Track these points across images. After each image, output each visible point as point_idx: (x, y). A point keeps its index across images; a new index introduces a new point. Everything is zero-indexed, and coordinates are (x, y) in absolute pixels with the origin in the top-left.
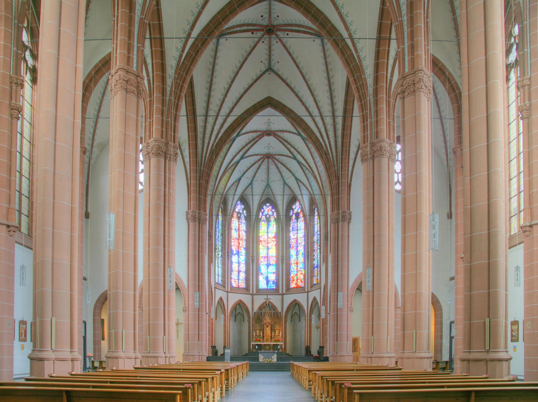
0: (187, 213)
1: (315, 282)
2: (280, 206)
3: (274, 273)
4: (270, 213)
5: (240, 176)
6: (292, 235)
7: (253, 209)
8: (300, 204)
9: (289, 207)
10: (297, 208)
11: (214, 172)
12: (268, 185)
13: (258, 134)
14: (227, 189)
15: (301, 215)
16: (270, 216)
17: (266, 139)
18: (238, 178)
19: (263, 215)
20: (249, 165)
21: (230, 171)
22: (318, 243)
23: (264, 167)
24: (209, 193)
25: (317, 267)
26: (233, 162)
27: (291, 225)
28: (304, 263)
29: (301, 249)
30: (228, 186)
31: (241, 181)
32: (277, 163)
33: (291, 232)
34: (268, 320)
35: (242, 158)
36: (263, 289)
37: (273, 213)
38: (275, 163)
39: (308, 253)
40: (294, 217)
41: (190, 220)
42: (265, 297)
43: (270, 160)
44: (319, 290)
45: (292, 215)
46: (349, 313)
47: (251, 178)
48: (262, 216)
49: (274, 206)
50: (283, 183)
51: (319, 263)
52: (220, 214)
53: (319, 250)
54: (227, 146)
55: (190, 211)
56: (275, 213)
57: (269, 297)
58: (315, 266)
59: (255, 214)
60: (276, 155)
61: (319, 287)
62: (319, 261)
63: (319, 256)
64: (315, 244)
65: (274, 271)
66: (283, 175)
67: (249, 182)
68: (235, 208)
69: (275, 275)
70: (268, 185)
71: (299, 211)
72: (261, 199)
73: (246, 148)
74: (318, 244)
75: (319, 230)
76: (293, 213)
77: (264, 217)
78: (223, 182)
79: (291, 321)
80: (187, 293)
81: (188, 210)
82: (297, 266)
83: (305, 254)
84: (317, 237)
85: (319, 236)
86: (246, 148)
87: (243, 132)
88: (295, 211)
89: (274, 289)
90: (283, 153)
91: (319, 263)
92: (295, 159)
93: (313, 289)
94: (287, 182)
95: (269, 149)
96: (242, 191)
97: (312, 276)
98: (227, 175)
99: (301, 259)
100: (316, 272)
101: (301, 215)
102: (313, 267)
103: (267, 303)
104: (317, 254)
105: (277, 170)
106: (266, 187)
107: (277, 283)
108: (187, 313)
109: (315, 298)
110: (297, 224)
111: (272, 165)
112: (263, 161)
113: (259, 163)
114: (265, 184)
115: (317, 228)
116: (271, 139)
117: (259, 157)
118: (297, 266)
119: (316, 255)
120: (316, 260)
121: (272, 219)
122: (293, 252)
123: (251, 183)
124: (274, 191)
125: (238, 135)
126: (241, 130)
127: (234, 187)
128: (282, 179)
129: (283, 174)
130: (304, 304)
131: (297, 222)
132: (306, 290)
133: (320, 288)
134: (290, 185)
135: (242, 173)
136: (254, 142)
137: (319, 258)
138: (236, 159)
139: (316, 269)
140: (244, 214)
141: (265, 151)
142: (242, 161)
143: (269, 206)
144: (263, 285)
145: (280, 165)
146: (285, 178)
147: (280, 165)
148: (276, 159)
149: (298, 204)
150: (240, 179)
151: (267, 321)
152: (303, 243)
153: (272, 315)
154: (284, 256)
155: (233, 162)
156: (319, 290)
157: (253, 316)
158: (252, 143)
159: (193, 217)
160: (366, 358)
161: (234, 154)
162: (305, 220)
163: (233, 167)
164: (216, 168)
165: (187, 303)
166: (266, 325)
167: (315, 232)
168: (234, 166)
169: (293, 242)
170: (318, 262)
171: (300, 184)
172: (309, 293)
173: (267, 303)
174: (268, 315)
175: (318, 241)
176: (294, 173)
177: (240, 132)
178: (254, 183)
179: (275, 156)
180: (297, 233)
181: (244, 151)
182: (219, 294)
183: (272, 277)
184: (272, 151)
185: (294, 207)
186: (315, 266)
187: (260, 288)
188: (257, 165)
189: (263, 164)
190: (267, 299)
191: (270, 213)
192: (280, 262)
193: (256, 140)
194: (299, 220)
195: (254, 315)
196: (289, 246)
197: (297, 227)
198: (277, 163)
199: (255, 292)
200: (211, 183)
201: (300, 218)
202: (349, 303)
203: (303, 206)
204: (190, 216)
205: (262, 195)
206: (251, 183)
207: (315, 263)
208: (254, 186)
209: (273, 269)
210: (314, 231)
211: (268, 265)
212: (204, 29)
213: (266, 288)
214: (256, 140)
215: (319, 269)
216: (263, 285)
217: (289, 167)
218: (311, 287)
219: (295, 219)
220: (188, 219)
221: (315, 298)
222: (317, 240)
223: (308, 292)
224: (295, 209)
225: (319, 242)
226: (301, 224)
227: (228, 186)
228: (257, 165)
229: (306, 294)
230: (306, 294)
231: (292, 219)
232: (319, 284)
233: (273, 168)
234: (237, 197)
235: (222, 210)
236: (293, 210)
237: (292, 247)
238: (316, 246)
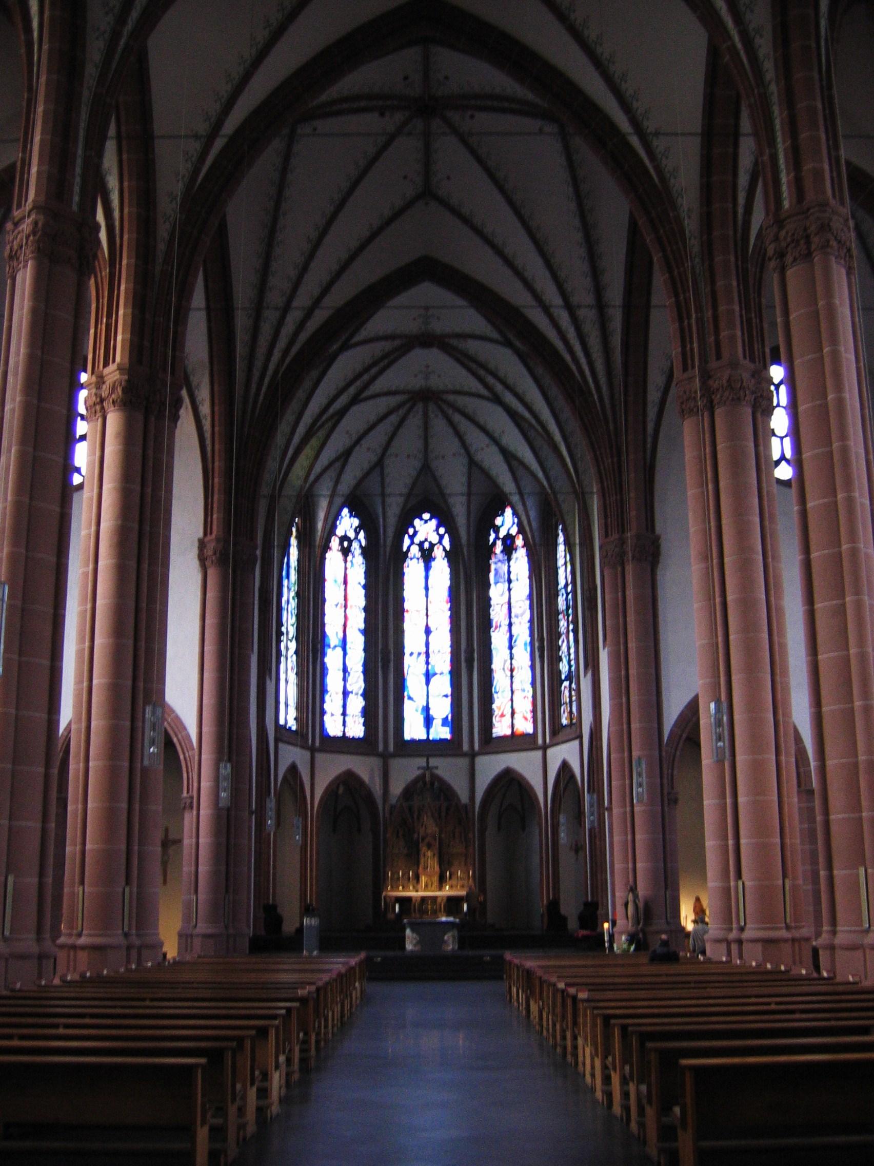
0: (202, 544)
1: (564, 721)
2: (461, 521)
3: (446, 696)
4: (434, 539)
5: (348, 443)
6: (497, 593)
7: (384, 527)
8: (515, 513)
9: (486, 523)
10: (507, 522)
11: (280, 439)
12: (426, 469)
13: (397, 342)
14: (312, 477)
15: (519, 542)
16: (432, 546)
17: (419, 357)
18: (341, 450)
19: (412, 543)
20: (373, 418)
21: (321, 434)
22: (568, 616)
23: (414, 422)
24: (265, 490)
25: (569, 677)
26: (331, 411)
27: (493, 567)
28: (533, 667)
29: (522, 631)
30: (318, 469)
31: (352, 459)
32: (450, 412)
33: (493, 586)
34: (429, 826)
35: (355, 400)
36: (413, 741)
37: (441, 537)
38: (443, 412)
39: (541, 640)
40: (499, 547)
41: (208, 563)
42: (422, 762)
43: (432, 407)
44: (577, 742)
45: (494, 543)
46: (666, 809)
47: (379, 451)
48: (409, 548)
49: (445, 519)
50: (465, 461)
51: (573, 669)
52: (293, 541)
53: (571, 635)
54: (314, 374)
55: (208, 538)
56: (446, 536)
57: (433, 762)
58: (563, 677)
59: (389, 541)
60: (447, 392)
61: (578, 733)
62: (573, 663)
63: (572, 650)
64: (561, 617)
65: (448, 691)
66: (468, 442)
67: (374, 458)
68: (334, 527)
69: (449, 700)
70: (426, 469)
71: (514, 531)
72: (406, 502)
73: (366, 377)
74: (570, 618)
75: (569, 581)
76: (497, 538)
77: (415, 550)
78: (303, 461)
79: (499, 829)
80: (196, 758)
81: (205, 534)
82: (512, 677)
83: (532, 643)
84: (567, 599)
85: (570, 596)
86: (366, 377)
87: (357, 338)
88: (503, 533)
89: (446, 740)
90: (466, 389)
91: (573, 669)
92: (497, 400)
93: (561, 737)
94: (478, 457)
95: (427, 378)
96: (353, 482)
97: (555, 703)
98: (314, 442)
99: (523, 657)
100: (567, 693)
101: (519, 542)
102: (555, 680)
103: (428, 779)
104: (566, 646)
105: (451, 431)
106: (421, 470)
107: (454, 722)
108: (195, 812)
109: (565, 766)
110: (509, 567)
111: (437, 416)
112: (411, 408)
113: (401, 412)
114: (417, 464)
115: (563, 576)
116: (434, 357)
117: (399, 399)
118: (512, 677)
119: (564, 648)
120: (565, 661)
121: (438, 553)
122: (498, 639)
123: (379, 464)
124: (444, 482)
125: (345, 347)
126: (352, 335)
127: (332, 473)
128: (462, 451)
129: (468, 439)
130: (536, 782)
131: (509, 560)
132: (540, 741)
133: (580, 737)
134: (486, 464)
135: (355, 437)
136: (386, 361)
137: (572, 656)
138: (337, 405)
139: (566, 683)
140: (360, 541)
141: (417, 383)
142: (355, 409)
143: (430, 519)
144: (414, 729)
145: (457, 418)
146: (472, 450)
147: (457, 418)
148: (445, 402)
149: (509, 512)
150: (346, 454)
151: (429, 831)
152: (527, 616)
153: (443, 814)
154: (473, 651)
155: (331, 411)
156: (577, 742)
157: (387, 815)
158: (382, 364)
159: (218, 555)
160: (724, 946)
161: (333, 392)
162: (530, 555)
163: (330, 424)
164: (283, 428)
165: (195, 784)
166: (427, 840)
167: (560, 587)
168: (333, 421)
169: (498, 614)
170: (570, 666)
171: (514, 463)
172: (550, 752)
173: (428, 779)
174: (429, 814)
175: (568, 608)
176: (496, 435)
177: (348, 339)
178: (387, 461)
179: (445, 397)
180: (509, 590)
181: (358, 383)
182: (291, 755)
183: (442, 708)
184: (435, 383)
185: (498, 521)
186: (563, 677)
187: (407, 736)
188: (394, 419)
189: (411, 414)
190: (428, 767)
191: (434, 539)
192: (463, 665)
193: (392, 357)
194: (514, 556)
195: (391, 814)
196: (486, 624)
197: (509, 573)
198: (450, 412)
199: (391, 748)
200: (272, 464)
201: (516, 550)
202: (665, 781)
203: (524, 518)
204: (209, 551)
205: (409, 496)
206: (379, 464)
207: (564, 667)
208: (386, 471)
209: (442, 684)
210: (558, 584)
211: (428, 676)
212: (258, 111)
213: (424, 737)
214: (392, 357)
215: (574, 686)
216: (414, 729)
217: (482, 421)
218: (554, 733)
219: (502, 552)
220: (202, 559)
221: (565, 766)
222: (564, 607)
223: (544, 748)
224: (502, 525)
225: (570, 611)
226: (520, 562)
227: (318, 469)
228: (394, 419)
229: (539, 754)
230: (539, 754)
231: (495, 554)
232: (575, 725)
233: (439, 425)
234: (338, 501)
235: (297, 530)
236: (497, 530)
237: (496, 628)
238: (563, 624)
